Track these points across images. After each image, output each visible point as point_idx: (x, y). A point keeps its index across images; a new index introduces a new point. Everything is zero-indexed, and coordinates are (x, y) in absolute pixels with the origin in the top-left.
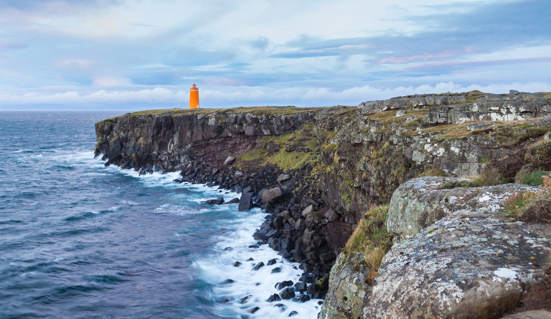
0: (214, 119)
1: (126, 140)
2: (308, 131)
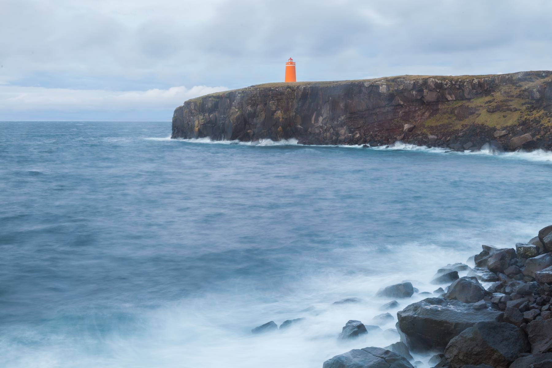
0: (384, 86)
1: (254, 115)
2: (508, 93)
